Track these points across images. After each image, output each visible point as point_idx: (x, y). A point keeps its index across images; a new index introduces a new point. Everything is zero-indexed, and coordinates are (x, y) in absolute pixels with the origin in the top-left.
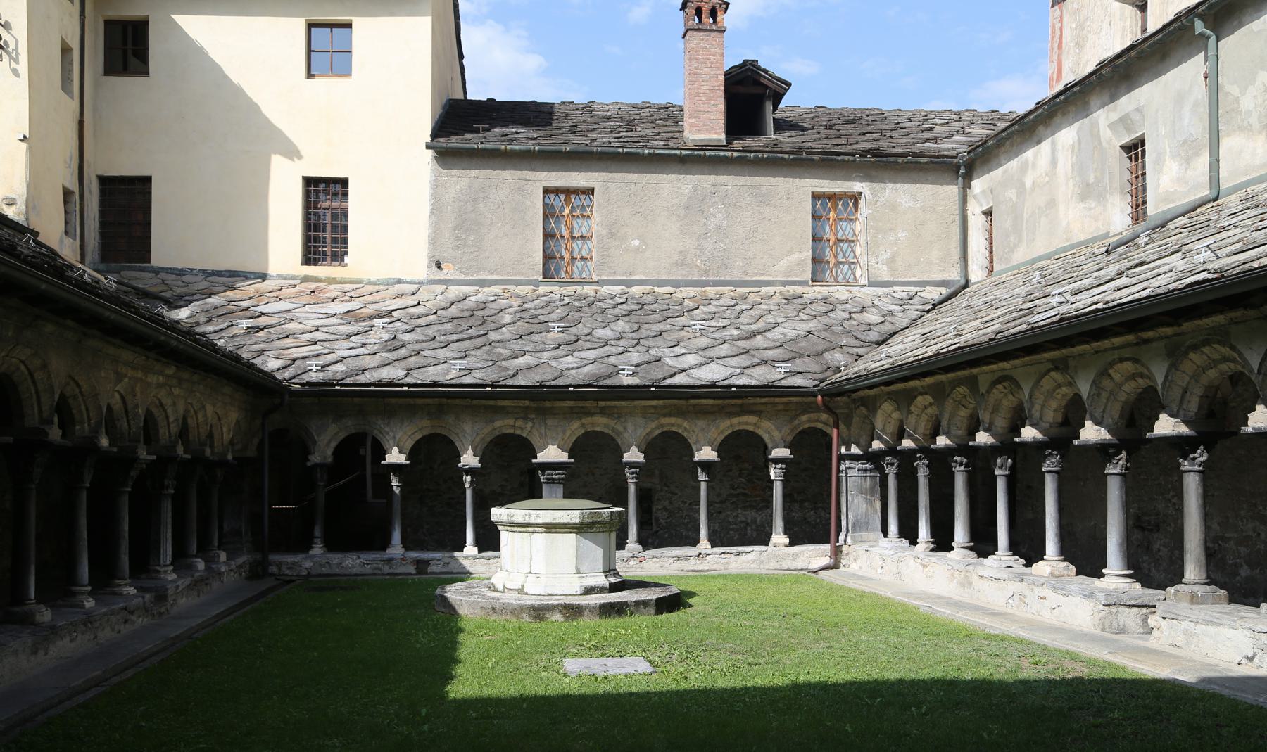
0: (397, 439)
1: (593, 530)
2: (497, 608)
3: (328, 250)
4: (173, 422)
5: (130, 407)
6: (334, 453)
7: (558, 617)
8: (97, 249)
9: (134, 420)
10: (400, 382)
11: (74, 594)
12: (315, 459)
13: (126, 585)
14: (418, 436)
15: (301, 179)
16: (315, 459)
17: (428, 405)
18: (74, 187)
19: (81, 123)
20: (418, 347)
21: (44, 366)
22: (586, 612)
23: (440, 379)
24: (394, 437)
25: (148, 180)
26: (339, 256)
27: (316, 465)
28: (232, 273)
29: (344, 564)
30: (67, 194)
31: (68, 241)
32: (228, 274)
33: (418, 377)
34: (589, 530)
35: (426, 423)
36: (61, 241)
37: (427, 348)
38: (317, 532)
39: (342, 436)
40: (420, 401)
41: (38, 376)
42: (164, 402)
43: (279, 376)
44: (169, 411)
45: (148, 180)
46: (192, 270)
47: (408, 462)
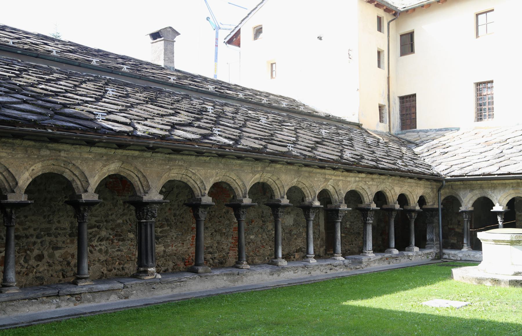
0: (498, 199)
1: (520, 244)
2: (464, 277)
3: (487, 114)
4: (370, 195)
5: (337, 190)
6: (474, 205)
7: (488, 284)
8: (399, 126)
9: (340, 195)
10: (493, 173)
11: (307, 257)
12: (462, 209)
13: (339, 256)
14: (510, 198)
15: (415, 93)
16: (462, 209)
17: (512, 183)
18: (385, 102)
19: (388, 78)
20: (510, 156)
21: (278, 179)
22: (502, 283)
23: (512, 171)
24: (497, 199)
25: (414, 95)
26: (491, 116)
27: (463, 212)
28: (446, 129)
29: (475, 256)
30: (381, 108)
31: (381, 124)
32: (444, 130)
33: (504, 170)
34: (518, 244)
35: (511, 191)
36: (378, 125)
37: (514, 156)
38: (465, 241)
39: (475, 198)
40: (507, 181)
41: (277, 182)
42: (364, 188)
43: (442, 173)
44: (367, 191)
45: (414, 95)
46: (431, 130)
47: (503, 210)
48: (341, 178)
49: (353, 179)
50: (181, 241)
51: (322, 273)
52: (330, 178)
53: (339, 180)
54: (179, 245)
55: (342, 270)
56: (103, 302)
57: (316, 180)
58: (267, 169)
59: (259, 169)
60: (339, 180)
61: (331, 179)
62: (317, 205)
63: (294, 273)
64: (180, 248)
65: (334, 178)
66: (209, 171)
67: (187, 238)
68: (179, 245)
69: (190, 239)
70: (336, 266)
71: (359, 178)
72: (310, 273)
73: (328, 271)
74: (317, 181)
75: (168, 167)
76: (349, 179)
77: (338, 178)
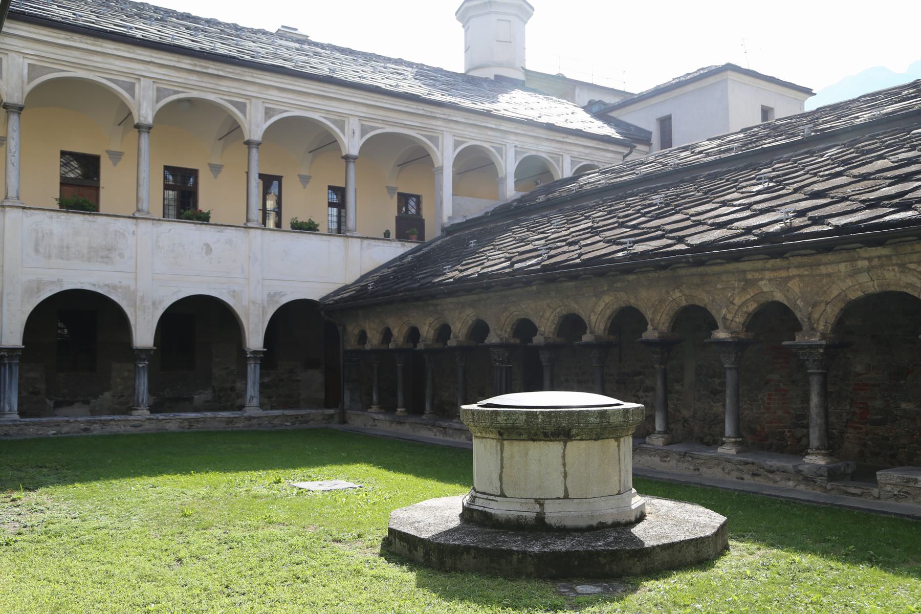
48: (793, 272)
49: (843, 267)
50: (748, 400)
51: (728, 477)
52: (760, 276)
53: (789, 278)
54: (745, 406)
55: (791, 483)
56: (457, 440)
57: (721, 287)
58: (615, 285)
59: (605, 289)
60: (789, 278)
61: (762, 279)
62: (721, 337)
63: (661, 461)
64: (747, 412)
65: (768, 275)
66: (539, 303)
67: (759, 397)
68: (745, 406)
69: (765, 398)
70: (772, 472)
71: (870, 259)
72: (699, 470)
73: (748, 478)
74: (722, 289)
75: (504, 305)
76: (823, 270)
77: (784, 274)
